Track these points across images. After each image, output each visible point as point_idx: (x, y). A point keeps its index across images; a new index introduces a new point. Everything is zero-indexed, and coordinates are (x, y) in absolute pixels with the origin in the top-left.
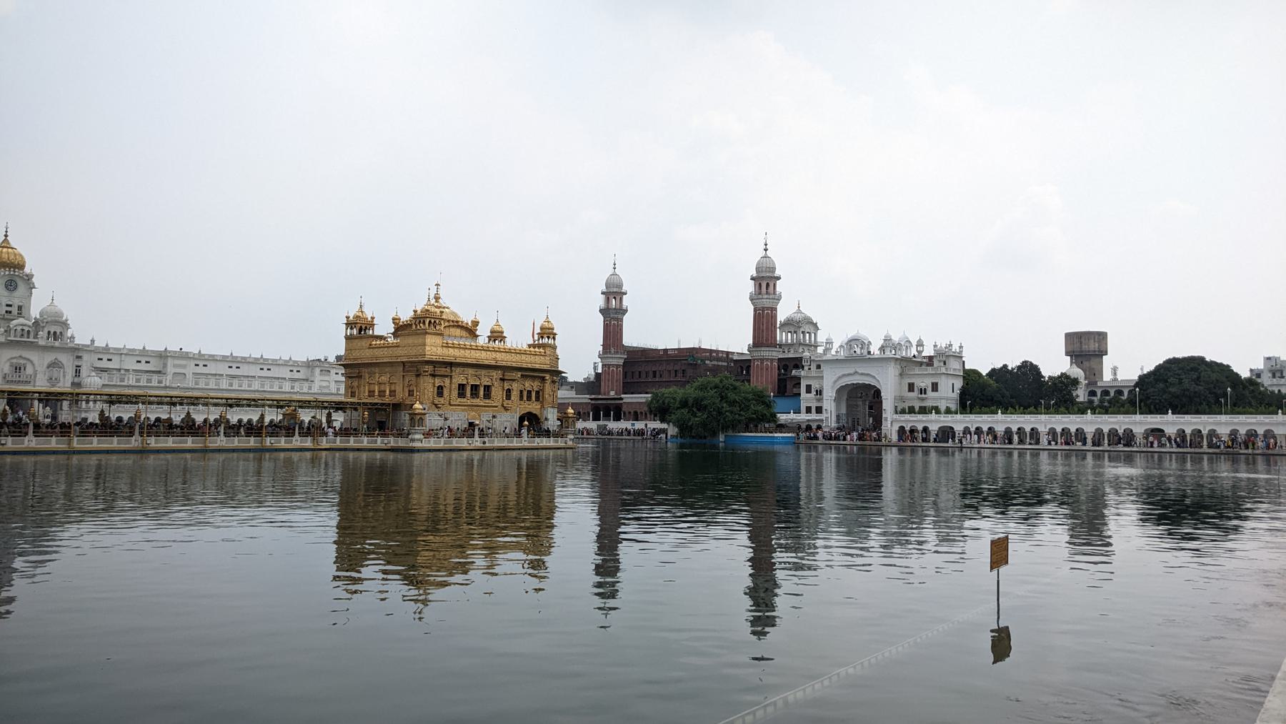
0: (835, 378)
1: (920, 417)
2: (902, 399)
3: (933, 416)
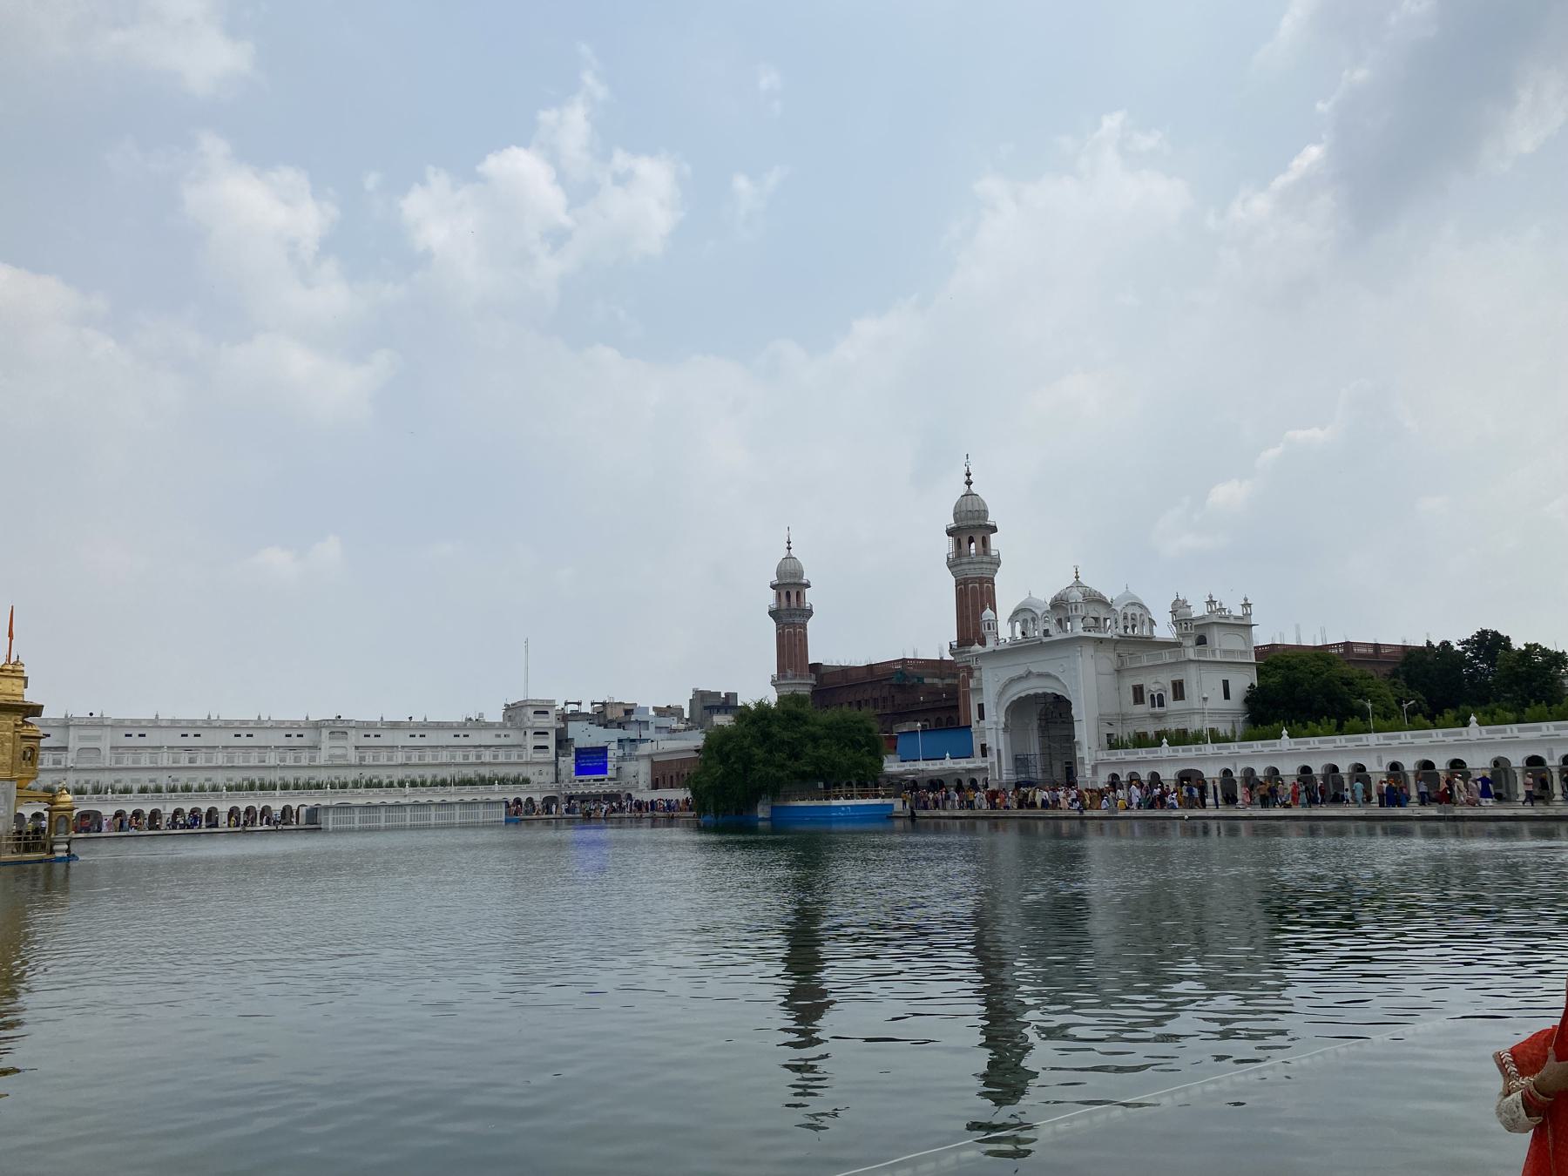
0: (998, 688)
1: (1142, 753)
2: (1124, 718)
3: (1165, 750)
